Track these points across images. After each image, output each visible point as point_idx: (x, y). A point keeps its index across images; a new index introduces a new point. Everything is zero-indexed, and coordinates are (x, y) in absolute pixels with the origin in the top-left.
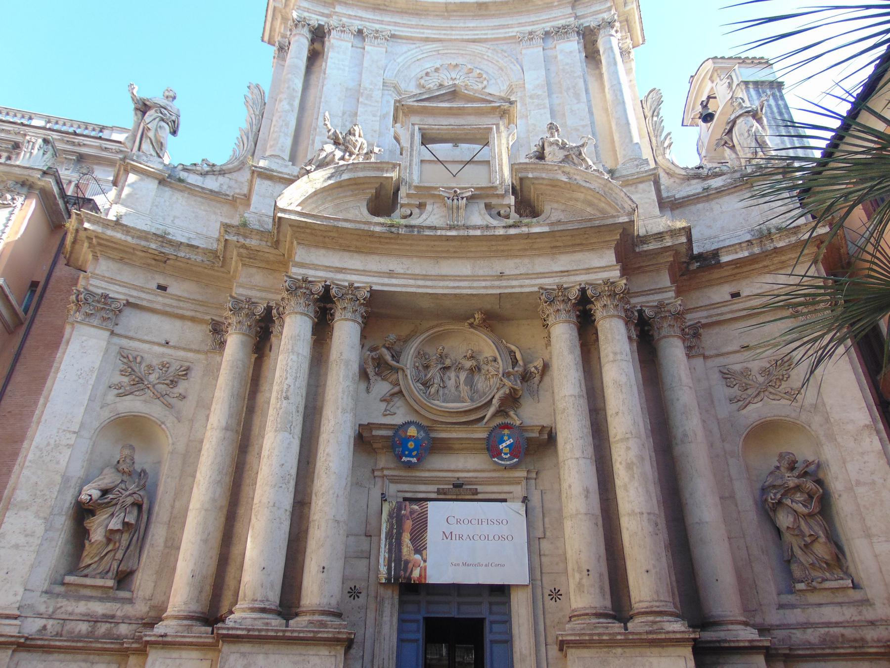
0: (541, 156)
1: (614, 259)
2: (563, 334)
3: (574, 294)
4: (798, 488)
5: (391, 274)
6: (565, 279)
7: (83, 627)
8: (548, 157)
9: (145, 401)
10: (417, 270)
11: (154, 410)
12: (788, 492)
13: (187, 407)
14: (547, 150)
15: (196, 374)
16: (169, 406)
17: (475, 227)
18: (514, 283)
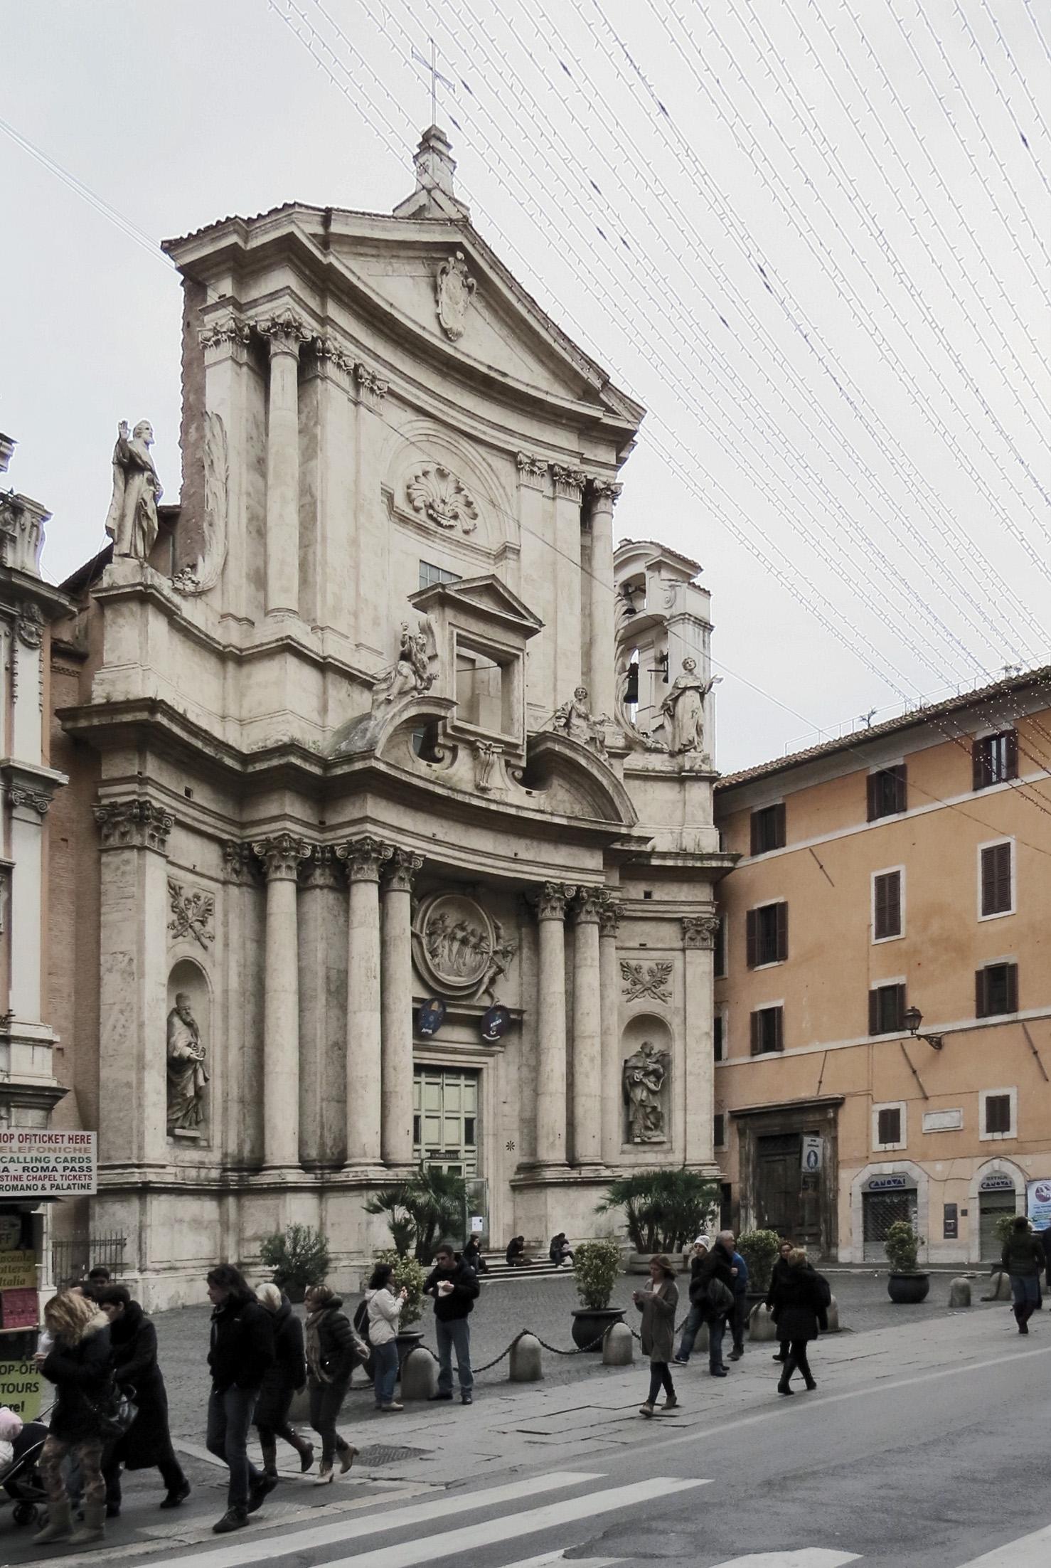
0: (567, 725)
1: (601, 861)
2: (554, 931)
3: (573, 893)
4: (654, 1072)
5: (433, 840)
6: (564, 874)
7: (193, 1173)
8: (574, 731)
9: (191, 944)
10: (452, 838)
11: (196, 953)
12: (647, 1074)
13: (217, 947)
14: (575, 721)
15: (218, 908)
16: (205, 948)
17: (511, 806)
18: (526, 868)
